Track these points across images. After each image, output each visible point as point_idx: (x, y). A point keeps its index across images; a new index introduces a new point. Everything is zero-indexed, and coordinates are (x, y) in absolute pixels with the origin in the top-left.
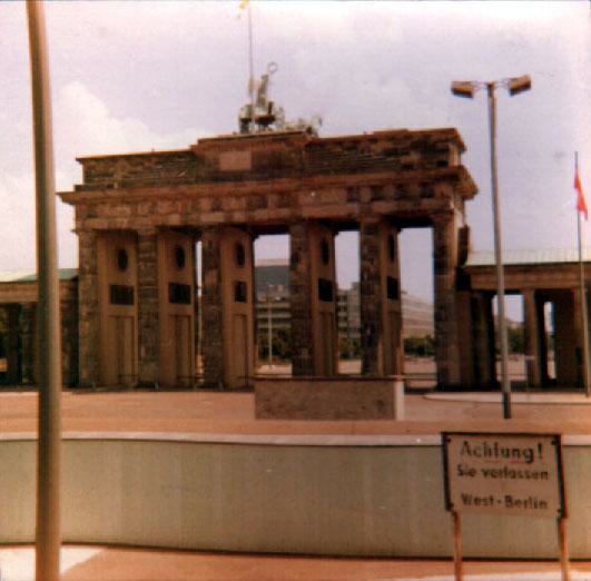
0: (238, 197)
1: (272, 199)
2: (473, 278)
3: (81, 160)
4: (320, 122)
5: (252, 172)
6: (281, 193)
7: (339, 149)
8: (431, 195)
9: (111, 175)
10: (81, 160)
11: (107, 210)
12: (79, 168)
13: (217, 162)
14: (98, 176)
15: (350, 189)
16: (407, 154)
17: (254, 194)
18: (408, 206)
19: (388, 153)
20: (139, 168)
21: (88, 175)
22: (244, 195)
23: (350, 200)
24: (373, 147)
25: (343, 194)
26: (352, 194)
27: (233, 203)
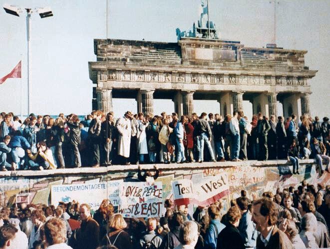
0: (206, 75)
1: (226, 79)
5: (213, 61)
6: (231, 76)
7: (255, 54)
9: (120, 52)
11: (121, 76)
13: (193, 53)
14: (110, 52)
15: (266, 77)
16: (286, 61)
19: (279, 59)
20: (138, 50)
22: (210, 74)
24: (271, 55)
27: (202, 79)
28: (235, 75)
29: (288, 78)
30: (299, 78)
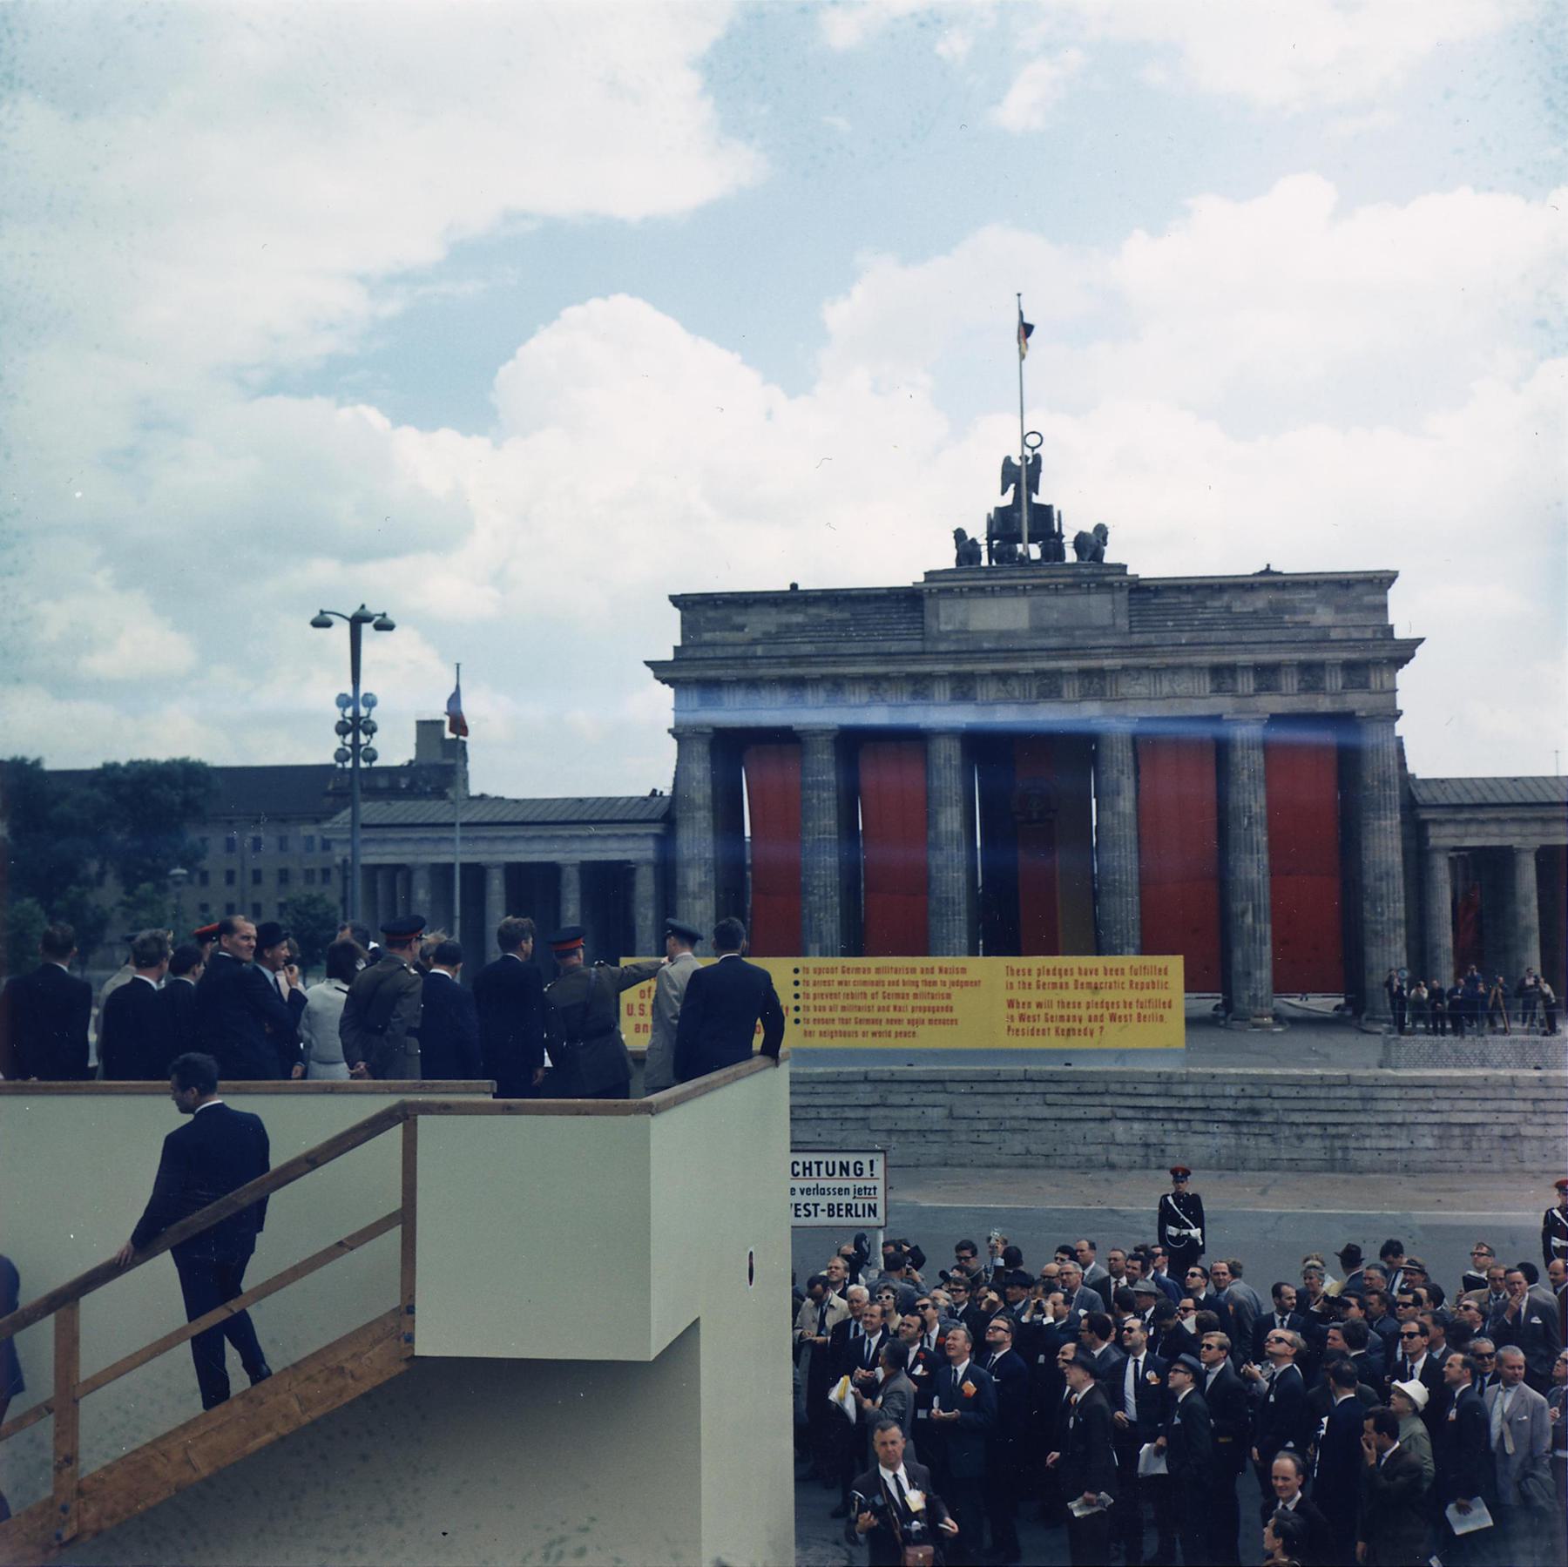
1: (1070, 689)
2: (1432, 830)
3: (676, 600)
4: (1105, 538)
6: (1085, 673)
8: (1364, 686)
9: (741, 628)
10: (676, 600)
12: (676, 614)
17: (1039, 674)
18: (1324, 704)
21: (687, 627)
22: (1016, 674)
23: (1218, 690)
25: (1206, 684)
26: (1222, 674)
28: (1101, 673)
29: (1306, 668)
30: (1349, 667)
